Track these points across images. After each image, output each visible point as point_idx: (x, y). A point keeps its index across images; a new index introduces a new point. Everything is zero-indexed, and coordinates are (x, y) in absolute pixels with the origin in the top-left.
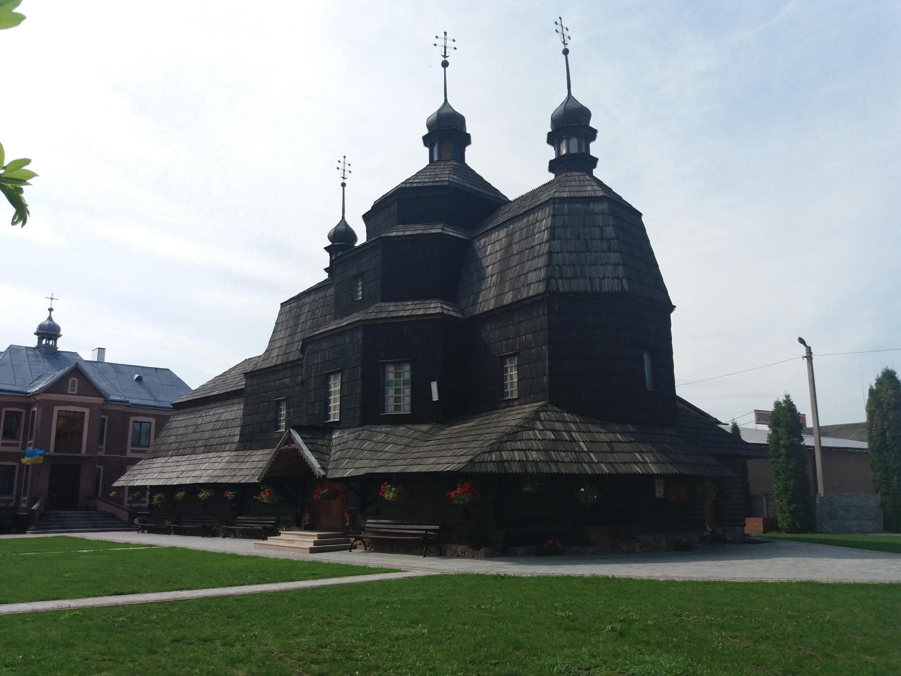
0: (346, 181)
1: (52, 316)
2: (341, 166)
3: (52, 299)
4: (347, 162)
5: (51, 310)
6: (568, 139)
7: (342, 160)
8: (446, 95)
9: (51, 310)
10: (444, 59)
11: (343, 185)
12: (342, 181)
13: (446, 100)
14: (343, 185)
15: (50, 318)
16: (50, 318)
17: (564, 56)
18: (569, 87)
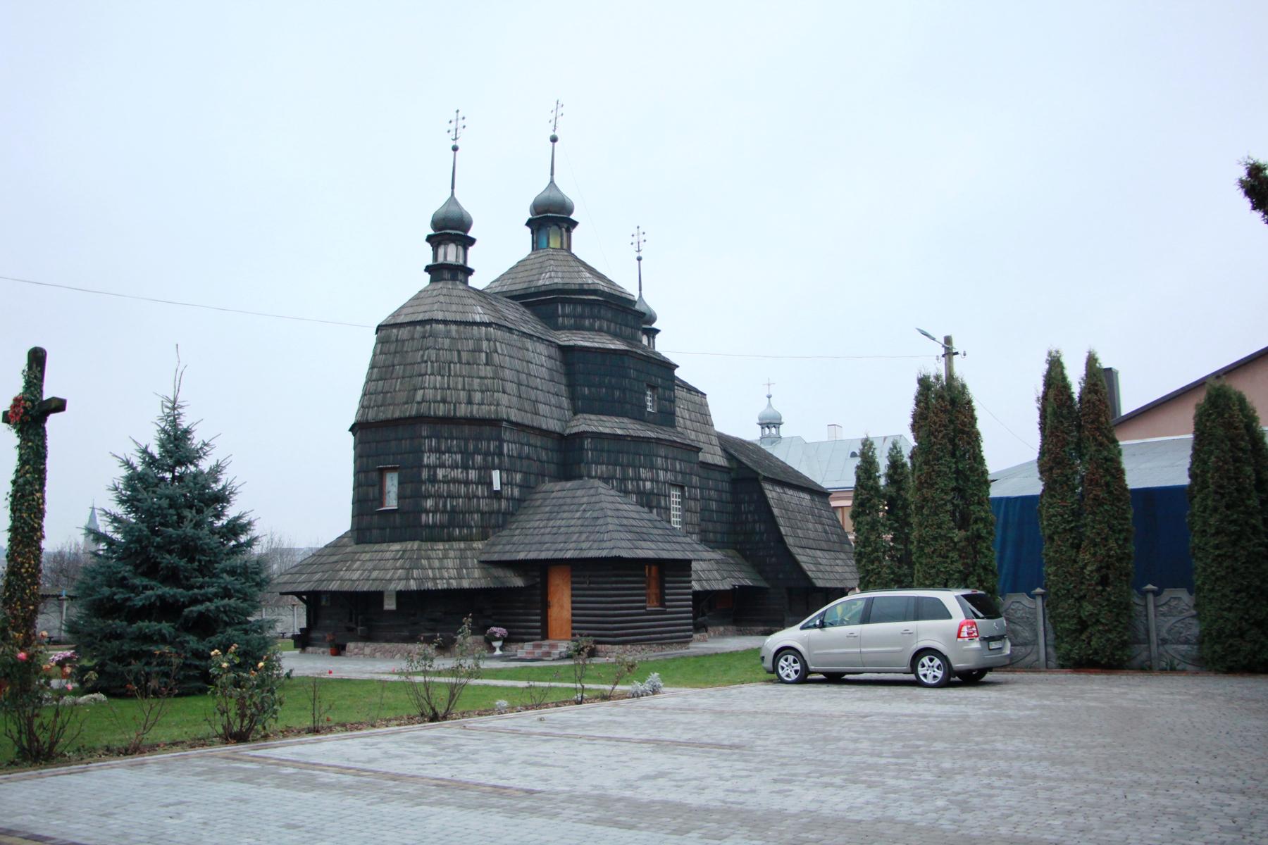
0: (641, 254)
1: (772, 402)
2: (635, 240)
3: (769, 385)
4: (641, 230)
5: (769, 397)
6: (446, 244)
7: (635, 231)
8: (552, 174)
9: (769, 397)
10: (552, 133)
11: (639, 259)
12: (637, 255)
13: (552, 182)
14: (639, 259)
15: (770, 405)
16: (770, 405)
17: (453, 152)
18: (453, 187)
